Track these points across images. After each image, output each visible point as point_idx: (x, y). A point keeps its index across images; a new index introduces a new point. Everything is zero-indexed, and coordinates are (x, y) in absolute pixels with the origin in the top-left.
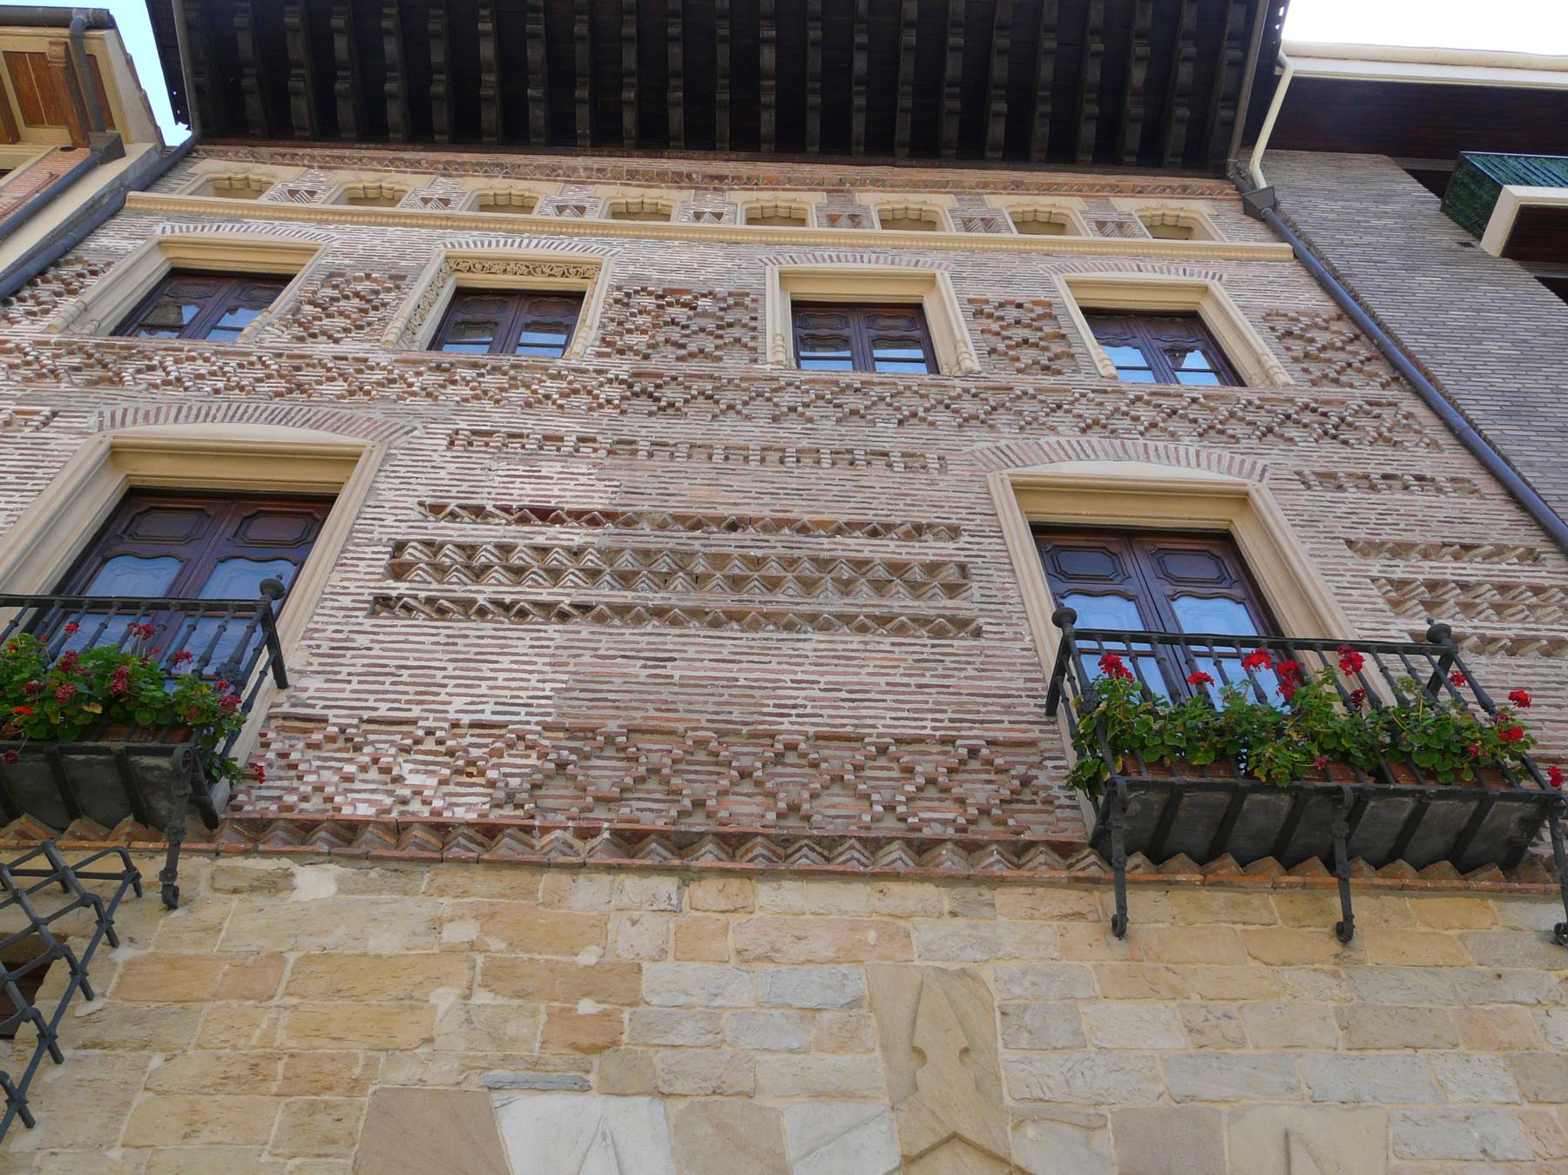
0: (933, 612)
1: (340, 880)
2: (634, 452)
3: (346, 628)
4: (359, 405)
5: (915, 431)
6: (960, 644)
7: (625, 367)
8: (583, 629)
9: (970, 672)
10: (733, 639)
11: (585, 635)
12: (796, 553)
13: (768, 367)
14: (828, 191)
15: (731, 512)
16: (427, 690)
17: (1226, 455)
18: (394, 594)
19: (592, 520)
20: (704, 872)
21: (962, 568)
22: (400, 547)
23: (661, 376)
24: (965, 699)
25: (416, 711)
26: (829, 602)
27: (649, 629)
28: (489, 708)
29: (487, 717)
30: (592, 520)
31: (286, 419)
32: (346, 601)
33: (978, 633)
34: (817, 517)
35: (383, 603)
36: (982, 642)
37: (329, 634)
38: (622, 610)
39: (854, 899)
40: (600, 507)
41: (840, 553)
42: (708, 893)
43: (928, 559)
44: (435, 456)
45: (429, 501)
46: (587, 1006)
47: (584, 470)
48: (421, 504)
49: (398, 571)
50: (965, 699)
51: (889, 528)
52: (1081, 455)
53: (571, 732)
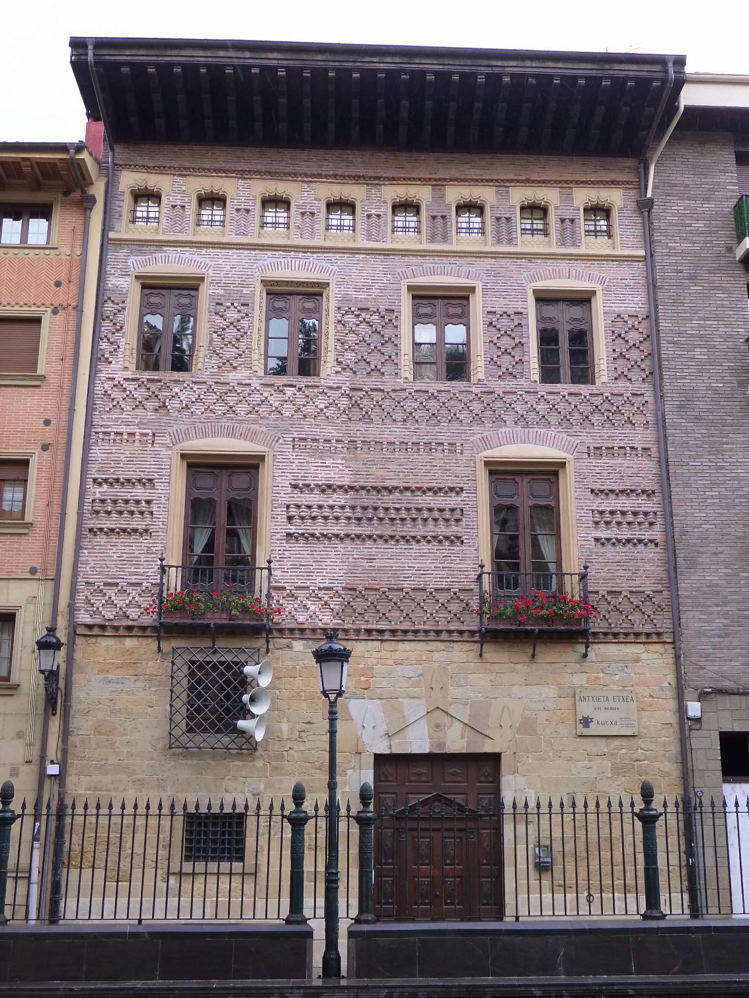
0: (450, 534)
1: (303, 645)
2: (356, 448)
3: (282, 549)
4: (255, 422)
5: (455, 426)
6: (457, 548)
7: (348, 385)
8: (348, 545)
9: (458, 561)
10: (393, 548)
11: (349, 549)
12: (410, 505)
13: (402, 381)
14: (432, 185)
15: (389, 484)
16: (310, 574)
17: (564, 435)
18: (292, 531)
19: (346, 489)
20: (386, 640)
21: (462, 510)
22: (288, 507)
23: (361, 390)
24: (456, 573)
25: (308, 583)
26: (420, 530)
27: (368, 546)
28: (327, 581)
29: (327, 585)
30: (346, 489)
31: (232, 434)
32: (278, 536)
33: (462, 542)
34: (418, 485)
35: (289, 535)
36: (463, 548)
37: (277, 552)
38: (358, 536)
39: (421, 646)
40: (348, 483)
41: (424, 505)
42: (387, 645)
43: (451, 507)
44: (290, 457)
45: (293, 482)
46: (363, 679)
47: (340, 462)
48: (290, 484)
49: (290, 518)
50: (456, 573)
51: (440, 489)
52: (511, 441)
53: (350, 589)
